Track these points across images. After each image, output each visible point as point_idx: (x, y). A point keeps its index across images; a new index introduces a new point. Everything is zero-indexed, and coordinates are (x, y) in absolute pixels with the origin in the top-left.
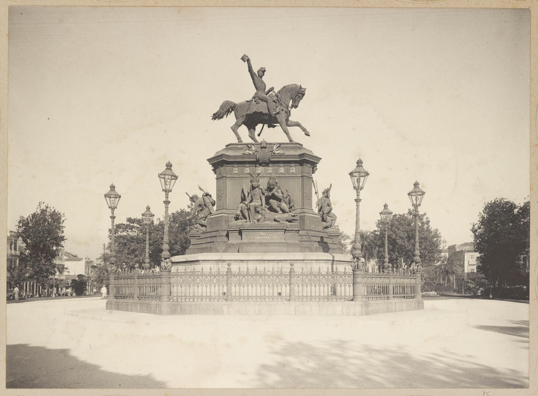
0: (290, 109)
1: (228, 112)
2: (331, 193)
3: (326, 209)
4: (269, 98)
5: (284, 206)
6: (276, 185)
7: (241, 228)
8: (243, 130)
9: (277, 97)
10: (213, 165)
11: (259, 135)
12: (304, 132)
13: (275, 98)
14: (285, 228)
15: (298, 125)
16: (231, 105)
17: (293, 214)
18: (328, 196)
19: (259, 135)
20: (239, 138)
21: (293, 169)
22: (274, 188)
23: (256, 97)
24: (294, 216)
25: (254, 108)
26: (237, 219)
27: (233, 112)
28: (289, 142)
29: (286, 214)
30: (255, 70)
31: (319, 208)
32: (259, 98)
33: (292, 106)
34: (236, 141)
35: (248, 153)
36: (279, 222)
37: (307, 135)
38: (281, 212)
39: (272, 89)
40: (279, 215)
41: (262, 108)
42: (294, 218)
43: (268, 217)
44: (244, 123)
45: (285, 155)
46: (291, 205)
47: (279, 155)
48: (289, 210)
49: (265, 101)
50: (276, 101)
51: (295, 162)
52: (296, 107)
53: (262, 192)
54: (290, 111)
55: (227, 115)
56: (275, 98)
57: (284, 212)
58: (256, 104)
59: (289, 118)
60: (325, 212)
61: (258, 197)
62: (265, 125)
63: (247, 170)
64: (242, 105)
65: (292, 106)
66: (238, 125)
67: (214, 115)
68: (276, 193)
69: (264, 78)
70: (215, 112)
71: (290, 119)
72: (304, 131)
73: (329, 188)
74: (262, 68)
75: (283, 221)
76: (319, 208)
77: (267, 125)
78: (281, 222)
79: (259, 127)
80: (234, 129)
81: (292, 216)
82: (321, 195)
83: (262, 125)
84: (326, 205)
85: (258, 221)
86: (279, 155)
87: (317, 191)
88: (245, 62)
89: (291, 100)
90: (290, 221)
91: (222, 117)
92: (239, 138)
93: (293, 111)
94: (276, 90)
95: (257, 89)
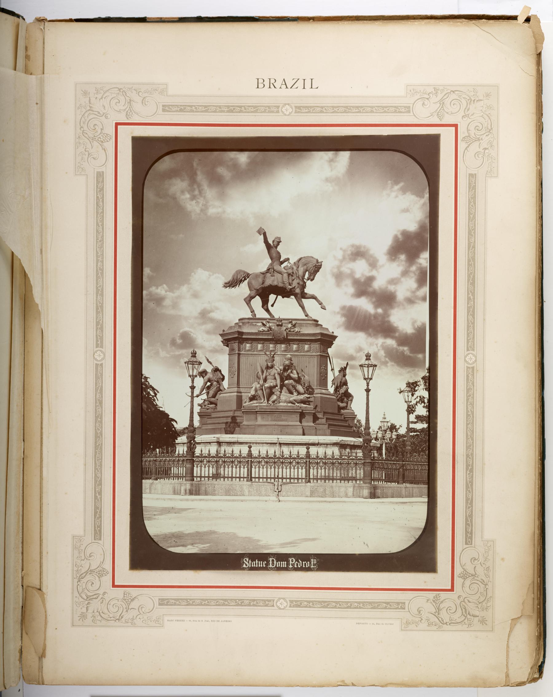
1: (241, 281)
11: (272, 306)
12: (320, 306)
19: (272, 306)
20: (253, 311)
25: (270, 281)
29: (302, 395)
30: (270, 242)
34: (249, 315)
36: (294, 404)
39: (288, 260)
43: (283, 398)
49: (280, 273)
52: (312, 280)
54: (305, 283)
55: (239, 284)
62: (279, 296)
64: (257, 276)
65: (308, 279)
66: (251, 298)
67: (226, 283)
69: (279, 249)
71: (306, 291)
73: (345, 366)
74: (277, 238)
75: (298, 403)
78: (297, 404)
80: (248, 300)
82: (337, 373)
88: (261, 235)
89: (307, 273)
92: (253, 311)
93: (308, 283)
94: (292, 261)
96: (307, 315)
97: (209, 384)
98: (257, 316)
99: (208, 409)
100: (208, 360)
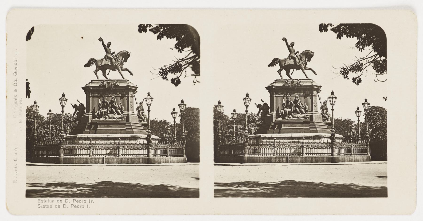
0: (123, 62)
8: (100, 73)
11: (108, 74)
27: (95, 63)
37: (132, 74)
41: (108, 62)
52: (126, 62)
55: (92, 65)
57: (118, 114)
58: (106, 60)
59: (123, 66)
62: (111, 70)
68: (115, 105)
71: (123, 67)
72: (130, 73)
89: (124, 58)
95: (106, 53)
98: (100, 79)
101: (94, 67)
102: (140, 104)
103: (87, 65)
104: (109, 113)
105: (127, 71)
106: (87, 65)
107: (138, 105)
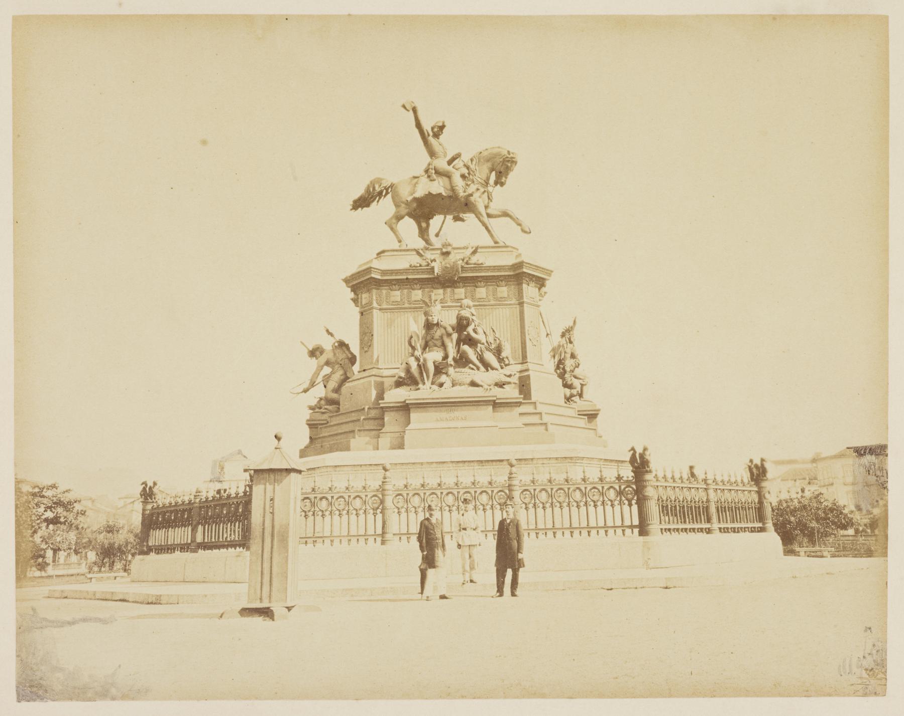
0: (490, 189)
2: (576, 335)
3: (569, 364)
4: (454, 170)
5: (490, 357)
6: (473, 319)
7: (407, 402)
8: (409, 226)
9: (468, 168)
10: (355, 289)
13: (465, 171)
14: (495, 399)
15: (505, 214)
16: (386, 185)
17: (508, 374)
18: (572, 340)
19: (437, 235)
21: (503, 291)
22: (468, 325)
23: (430, 170)
24: (510, 376)
26: (399, 384)
27: (389, 196)
28: (492, 244)
30: (427, 127)
31: (555, 362)
32: (435, 169)
33: (496, 183)
35: (418, 265)
38: (482, 368)
40: (481, 376)
41: (438, 187)
42: (508, 379)
44: (410, 215)
45: (486, 267)
46: (504, 355)
47: (475, 266)
48: (500, 366)
50: (467, 175)
51: (507, 279)
53: (446, 332)
55: (378, 201)
56: (465, 171)
58: (431, 180)
60: (568, 369)
61: (439, 343)
62: (448, 217)
63: (417, 294)
66: (399, 218)
67: (355, 202)
68: (473, 334)
70: (356, 197)
75: (490, 386)
76: (556, 363)
77: (451, 217)
79: (436, 221)
81: (505, 375)
83: (442, 217)
84: (568, 356)
85: (441, 385)
86: (475, 266)
87: (549, 333)
89: (494, 173)
90: (500, 385)
91: (368, 205)
94: (466, 158)
96: (496, 242)
97: (327, 370)
99: (323, 413)
100: (327, 331)
101: (385, 207)
102: (563, 335)
103: (362, 203)
104: (452, 363)
105: (508, 219)
106: (362, 203)
107: (557, 339)
